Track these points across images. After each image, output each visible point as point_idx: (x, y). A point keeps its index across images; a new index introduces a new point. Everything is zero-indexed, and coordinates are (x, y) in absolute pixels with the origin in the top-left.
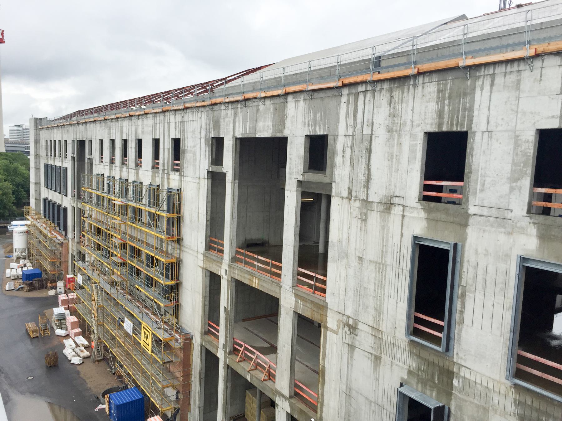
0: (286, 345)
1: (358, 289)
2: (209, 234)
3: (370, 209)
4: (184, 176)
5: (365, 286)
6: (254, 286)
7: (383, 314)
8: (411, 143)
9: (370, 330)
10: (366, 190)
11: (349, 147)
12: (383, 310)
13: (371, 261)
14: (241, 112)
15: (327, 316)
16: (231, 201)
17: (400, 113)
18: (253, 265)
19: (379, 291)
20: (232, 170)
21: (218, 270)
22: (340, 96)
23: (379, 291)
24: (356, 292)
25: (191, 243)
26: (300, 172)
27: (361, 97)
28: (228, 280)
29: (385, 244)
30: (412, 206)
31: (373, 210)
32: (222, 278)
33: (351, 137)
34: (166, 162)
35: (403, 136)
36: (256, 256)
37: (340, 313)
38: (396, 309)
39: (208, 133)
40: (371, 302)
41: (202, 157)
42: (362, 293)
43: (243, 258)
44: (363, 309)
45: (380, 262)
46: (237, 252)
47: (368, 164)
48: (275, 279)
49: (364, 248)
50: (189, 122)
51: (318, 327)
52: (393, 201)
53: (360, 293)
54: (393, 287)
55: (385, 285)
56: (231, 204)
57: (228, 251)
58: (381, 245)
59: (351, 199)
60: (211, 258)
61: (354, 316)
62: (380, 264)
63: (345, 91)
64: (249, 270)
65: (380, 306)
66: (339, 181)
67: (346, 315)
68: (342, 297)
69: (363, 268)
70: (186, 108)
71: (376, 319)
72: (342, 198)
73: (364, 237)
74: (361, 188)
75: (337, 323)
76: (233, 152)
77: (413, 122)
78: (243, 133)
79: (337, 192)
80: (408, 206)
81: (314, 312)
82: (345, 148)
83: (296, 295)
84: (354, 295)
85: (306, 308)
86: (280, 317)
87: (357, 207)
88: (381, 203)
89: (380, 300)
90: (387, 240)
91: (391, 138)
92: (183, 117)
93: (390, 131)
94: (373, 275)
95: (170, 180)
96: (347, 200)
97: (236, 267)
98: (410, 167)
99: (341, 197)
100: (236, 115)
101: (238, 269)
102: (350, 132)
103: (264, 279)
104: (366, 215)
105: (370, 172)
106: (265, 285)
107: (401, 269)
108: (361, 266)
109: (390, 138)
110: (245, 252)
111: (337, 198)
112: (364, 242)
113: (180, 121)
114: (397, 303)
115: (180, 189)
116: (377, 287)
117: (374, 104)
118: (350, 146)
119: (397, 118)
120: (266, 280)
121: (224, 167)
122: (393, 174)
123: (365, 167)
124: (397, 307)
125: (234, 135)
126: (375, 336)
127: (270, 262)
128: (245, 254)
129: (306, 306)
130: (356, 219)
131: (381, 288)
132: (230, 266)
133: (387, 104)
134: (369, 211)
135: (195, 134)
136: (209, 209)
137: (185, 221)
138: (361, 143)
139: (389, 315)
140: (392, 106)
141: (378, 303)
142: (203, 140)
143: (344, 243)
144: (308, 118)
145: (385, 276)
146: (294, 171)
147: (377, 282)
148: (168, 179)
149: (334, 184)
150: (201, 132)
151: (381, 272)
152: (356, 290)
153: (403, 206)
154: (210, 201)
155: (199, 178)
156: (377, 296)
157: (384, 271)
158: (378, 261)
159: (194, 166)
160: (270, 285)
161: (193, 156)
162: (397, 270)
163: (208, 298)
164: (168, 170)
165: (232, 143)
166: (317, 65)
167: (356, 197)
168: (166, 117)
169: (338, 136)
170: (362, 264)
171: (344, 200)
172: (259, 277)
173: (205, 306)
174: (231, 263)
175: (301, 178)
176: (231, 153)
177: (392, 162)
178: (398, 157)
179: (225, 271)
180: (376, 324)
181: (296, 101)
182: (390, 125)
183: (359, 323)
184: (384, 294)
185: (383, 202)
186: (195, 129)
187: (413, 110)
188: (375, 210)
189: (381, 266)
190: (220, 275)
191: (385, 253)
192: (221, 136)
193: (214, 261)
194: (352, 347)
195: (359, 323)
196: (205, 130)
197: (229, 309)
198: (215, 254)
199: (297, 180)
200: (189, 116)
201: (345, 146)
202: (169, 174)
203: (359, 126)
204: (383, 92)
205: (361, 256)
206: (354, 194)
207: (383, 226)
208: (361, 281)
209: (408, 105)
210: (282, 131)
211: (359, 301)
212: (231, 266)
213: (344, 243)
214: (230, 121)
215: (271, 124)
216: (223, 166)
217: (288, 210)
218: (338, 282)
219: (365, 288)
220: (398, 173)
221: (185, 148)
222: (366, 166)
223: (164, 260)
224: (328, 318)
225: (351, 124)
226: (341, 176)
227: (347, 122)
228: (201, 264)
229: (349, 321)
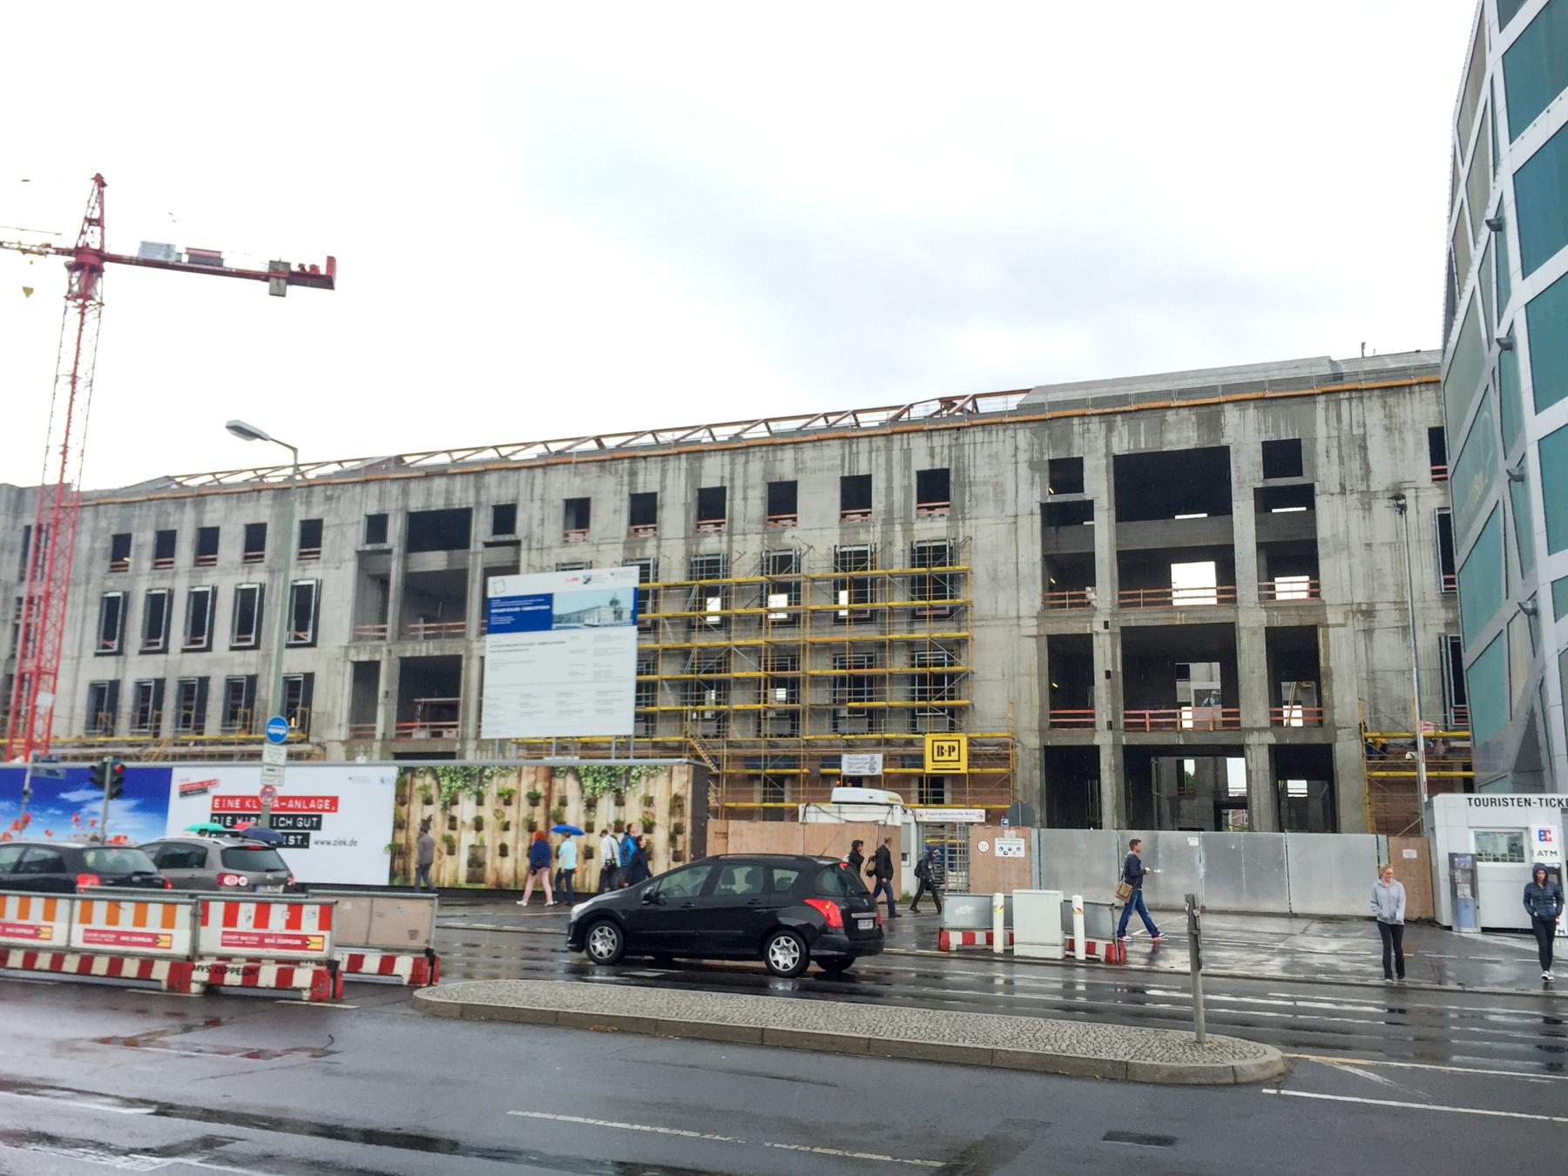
0: (1256, 670)
9: (1393, 606)
13: (1382, 544)
14: (1123, 425)
22: (1315, 402)
27: (1345, 406)
40: (1390, 580)
42: (1376, 576)
46: (1121, 597)
63: (1322, 399)
68: (1346, 588)
72: (1332, 494)
76: (1107, 472)
84: (1364, 580)
92: (956, 439)
93: (1388, 429)
102: (1334, 433)
104: (1370, 504)
126: (1400, 609)
142: (1023, 469)
143: (1342, 537)
149: (1317, 484)
150: (1015, 456)
155: (1016, 516)
166: (1277, 375)
167: (1352, 490)
181: (1240, 410)
194: (1369, 632)
204: (1374, 399)
206: (1348, 487)
210: (1218, 440)
221: (967, 480)
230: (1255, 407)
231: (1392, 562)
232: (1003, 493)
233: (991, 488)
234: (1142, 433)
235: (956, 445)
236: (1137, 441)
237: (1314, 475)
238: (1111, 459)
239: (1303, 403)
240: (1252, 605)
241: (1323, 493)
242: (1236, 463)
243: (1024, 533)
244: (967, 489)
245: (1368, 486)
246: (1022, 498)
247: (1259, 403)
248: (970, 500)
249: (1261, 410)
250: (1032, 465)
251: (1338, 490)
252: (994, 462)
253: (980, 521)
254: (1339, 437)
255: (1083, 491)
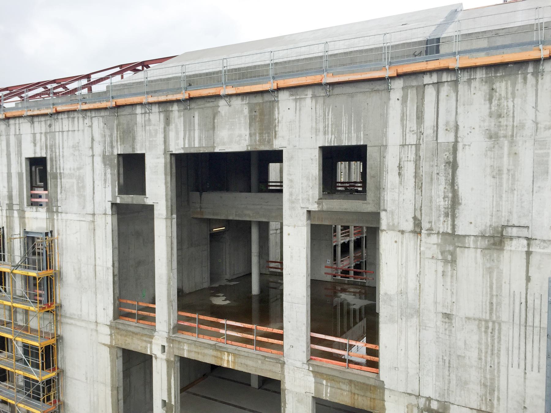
1: (445, 358)
2: (117, 295)
3: (460, 245)
4: (57, 212)
5: (459, 354)
6: (225, 365)
7: (499, 390)
8: (536, 152)
10: (450, 219)
11: (410, 161)
12: (498, 386)
13: (468, 319)
14: (179, 117)
15: (384, 401)
16: (167, 245)
17: (512, 112)
18: (219, 335)
19: (489, 359)
20: (167, 200)
21: (146, 348)
22: (389, 90)
23: (489, 359)
24: (441, 363)
25: (81, 311)
26: (313, 198)
27: (430, 92)
28: (168, 361)
29: (494, 293)
30: (545, 238)
31: (467, 246)
32: (154, 359)
33: (414, 147)
34: (15, 193)
35: (520, 143)
36: (223, 321)
37: (410, 394)
38: (525, 382)
39: (108, 149)
40: (474, 375)
41: (99, 183)
42: (454, 363)
43: (196, 325)
44: (457, 386)
45: (488, 318)
46: (180, 318)
47: (453, 183)
48: (274, 353)
49: (454, 300)
50: (65, 133)
51: (258, 389)
52: (507, 233)
53: (449, 363)
54: (516, 351)
55: (499, 351)
56: (167, 251)
57: (166, 318)
58: (489, 295)
59: (420, 233)
60: (127, 331)
61: (439, 397)
62: (486, 321)
63: (398, 84)
64: (212, 343)
65: (492, 379)
66: (393, 208)
67: (423, 397)
68: (412, 372)
69: (453, 329)
70: (58, 113)
71: (486, 399)
72: (403, 232)
73: (452, 286)
74: (439, 216)
75: (406, 410)
77: (537, 124)
78: (187, 146)
79: (391, 224)
80: (538, 238)
81: (356, 397)
82: (402, 163)
83: (316, 374)
85: (339, 391)
86: (285, 407)
87: (434, 244)
88: (483, 236)
89: (492, 372)
90: (500, 288)
91: (496, 146)
92: (50, 126)
93: (493, 136)
94: (475, 338)
95: (27, 220)
96: (412, 235)
97: (185, 341)
98: (536, 185)
99: (399, 231)
100: (167, 121)
101: (188, 344)
102: (412, 139)
103: (243, 353)
104: (453, 254)
105: (458, 195)
106: (250, 363)
107: (530, 326)
108: (449, 326)
109: (494, 147)
110: (198, 316)
111: (391, 233)
112: (453, 293)
113: (43, 131)
114: (525, 373)
115: (51, 232)
116: (483, 354)
117: (457, 101)
118: (412, 159)
119: (505, 118)
120: (250, 355)
121: (147, 196)
122: (504, 195)
123: (445, 188)
124: (525, 378)
125: (165, 151)
127: (255, 328)
128: (198, 318)
129: (339, 389)
130: (434, 261)
131: (492, 354)
132: (170, 340)
133: (485, 100)
134: (458, 249)
135: (79, 150)
136: (116, 259)
137: (64, 279)
138: (436, 153)
139: (510, 391)
140: (495, 102)
141: (488, 376)
142: (98, 160)
143: (411, 296)
144: (324, 122)
145: (499, 338)
146: (300, 197)
147: (483, 347)
148: (22, 217)
149: (383, 215)
150: (92, 148)
151: (491, 333)
152: (441, 360)
153: (528, 239)
154: (117, 246)
155: (94, 214)
156: (486, 366)
157: (496, 331)
158: (484, 317)
159: (82, 196)
160: (260, 362)
161: (78, 183)
162: (523, 328)
163: (121, 389)
164: (21, 204)
165: (164, 162)
167: (430, 229)
168: (12, 128)
169: (386, 146)
170: (451, 323)
171: (406, 235)
172: (236, 352)
173: (118, 401)
174: (174, 336)
175: (314, 207)
176: (163, 176)
177: (501, 179)
178: (511, 172)
179: (160, 348)
180: (486, 406)
181: (296, 100)
182: (492, 129)
183: (451, 406)
184: (499, 363)
185: (487, 235)
186: (78, 143)
187: (536, 107)
188: (472, 245)
189: (490, 324)
190: (149, 353)
191: (497, 306)
192: (139, 152)
193: (137, 334)
195: (451, 406)
196: (102, 144)
197: (173, 403)
198: (134, 324)
199: (307, 211)
200: (64, 123)
201: (403, 160)
202: (24, 211)
203: (428, 130)
204: (474, 84)
205: (448, 312)
206: (425, 225)
207: (490, 268)
208: (450, 347)
209: (525, 101)
210: (270, 142)
211: (449, 376)
212: (173, 340)
213: (411, 296)
214: (156, 131)
215: (248, 132)
216: (145, 195)
217: (291, 253)
218: (404, 350)
219: (459, 356)
220: (513, 194)
221: (58, 171)
222: (447, 187)
223: (36, 344)
224: (386, 403)
225: (412, 129)
226: (397, 202)
227: (403, 126)
228: (107, 340)
229: (431, 405)
230: (314, 97)
231: (480, 350)
232: (84, 187)
233: (74, 181)
234: (197, 127)
235: (50, 132)
236: (191, 139)
237: (378, 201)
238: (168, 156)
239: (373, 91)
240: (299, 364)
241: (392, 228)
242: (289, 174)
243: (100, 233)
244: (59, 180)
245: (454, 226)
246: (98, 197)
247: (320, 92)
248: (61, 192)
249: (321, 101)
250: (105, 159)
251: (409, 226)
252: (77, 153)
253: (69, 216)
254: (417, 146)
255: (146, 195)
